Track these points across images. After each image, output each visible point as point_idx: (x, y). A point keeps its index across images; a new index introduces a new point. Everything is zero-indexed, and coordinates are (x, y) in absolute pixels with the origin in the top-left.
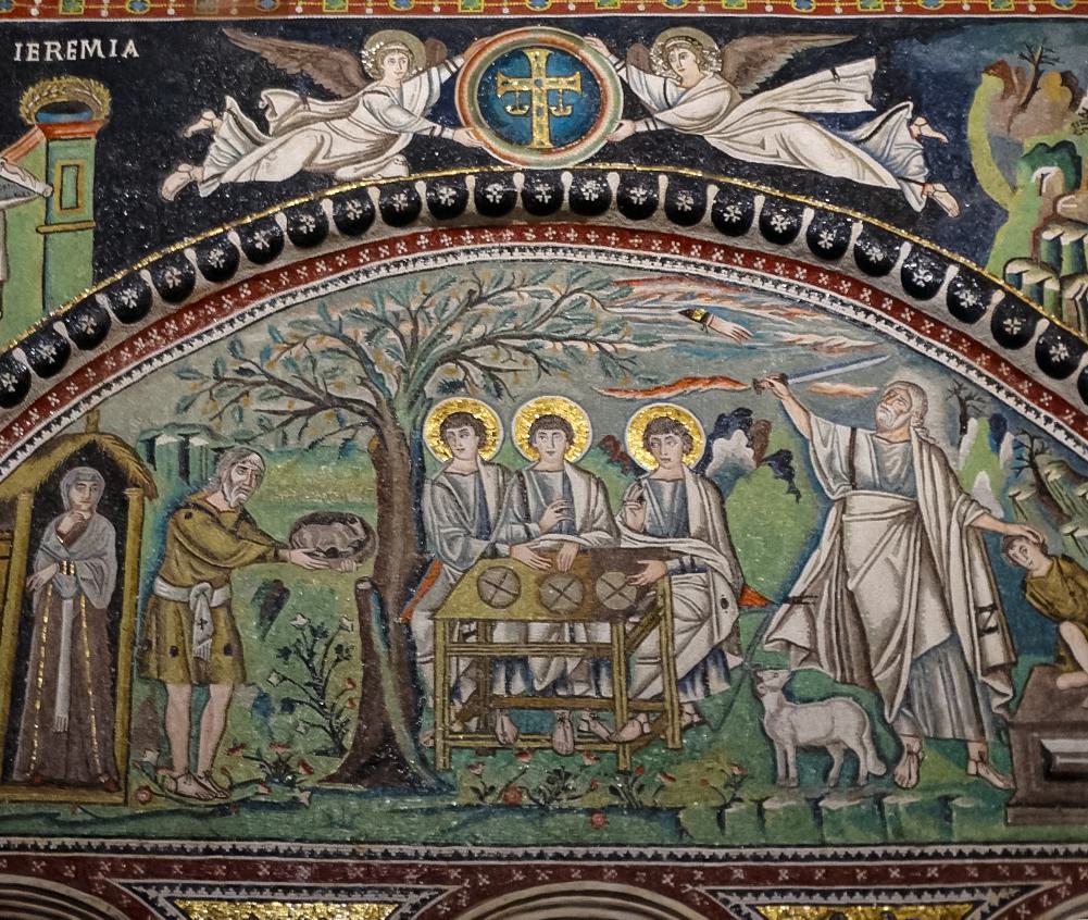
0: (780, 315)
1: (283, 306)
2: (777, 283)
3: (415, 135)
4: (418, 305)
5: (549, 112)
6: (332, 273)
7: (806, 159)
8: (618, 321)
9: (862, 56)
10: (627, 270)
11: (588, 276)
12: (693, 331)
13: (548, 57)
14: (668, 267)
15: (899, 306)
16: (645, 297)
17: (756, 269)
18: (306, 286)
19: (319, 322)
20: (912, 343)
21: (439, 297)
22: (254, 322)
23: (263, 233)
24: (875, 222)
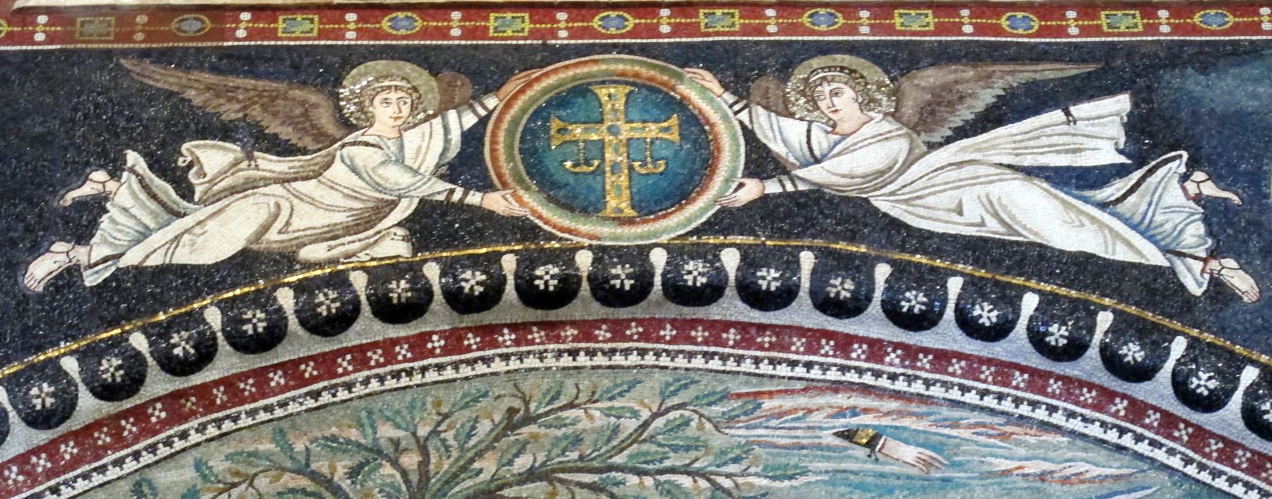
0: (990, 436)
1: (217, 432)
2: (983, 394)
3: (422, 201)
4: (428, 429)
5: (631, 168)
6: (294, 388)
7: (1025, 227)
8: (739, 446)
9: (1110, 92)
10: (754, 380)
11: (693, 387)
12: (857, 459)
13: (628, 95)
14: (816, 373)
15: (1169, 422)
16: (780, 415)
17: (953, 374)
18: (253, 406)
19: (273, 454)
20: (1191, 470)
21: (462, 417)
22: (172, 455)
23: (185, 334)
24: (1133, 310)
